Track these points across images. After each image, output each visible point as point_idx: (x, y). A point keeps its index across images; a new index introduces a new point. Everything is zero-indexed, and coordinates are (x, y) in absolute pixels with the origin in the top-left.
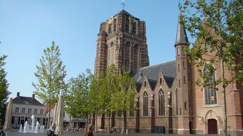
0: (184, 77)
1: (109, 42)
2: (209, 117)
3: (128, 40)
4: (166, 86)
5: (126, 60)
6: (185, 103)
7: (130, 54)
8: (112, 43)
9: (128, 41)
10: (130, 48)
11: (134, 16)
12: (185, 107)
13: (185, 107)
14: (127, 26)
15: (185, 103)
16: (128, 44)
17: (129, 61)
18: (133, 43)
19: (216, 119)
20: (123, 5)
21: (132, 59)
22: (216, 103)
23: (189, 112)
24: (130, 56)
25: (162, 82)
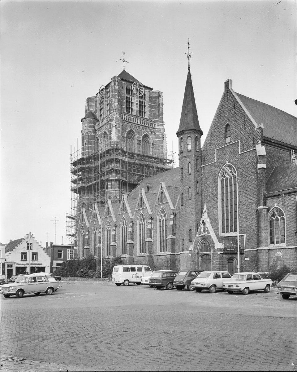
20: (124, 61)
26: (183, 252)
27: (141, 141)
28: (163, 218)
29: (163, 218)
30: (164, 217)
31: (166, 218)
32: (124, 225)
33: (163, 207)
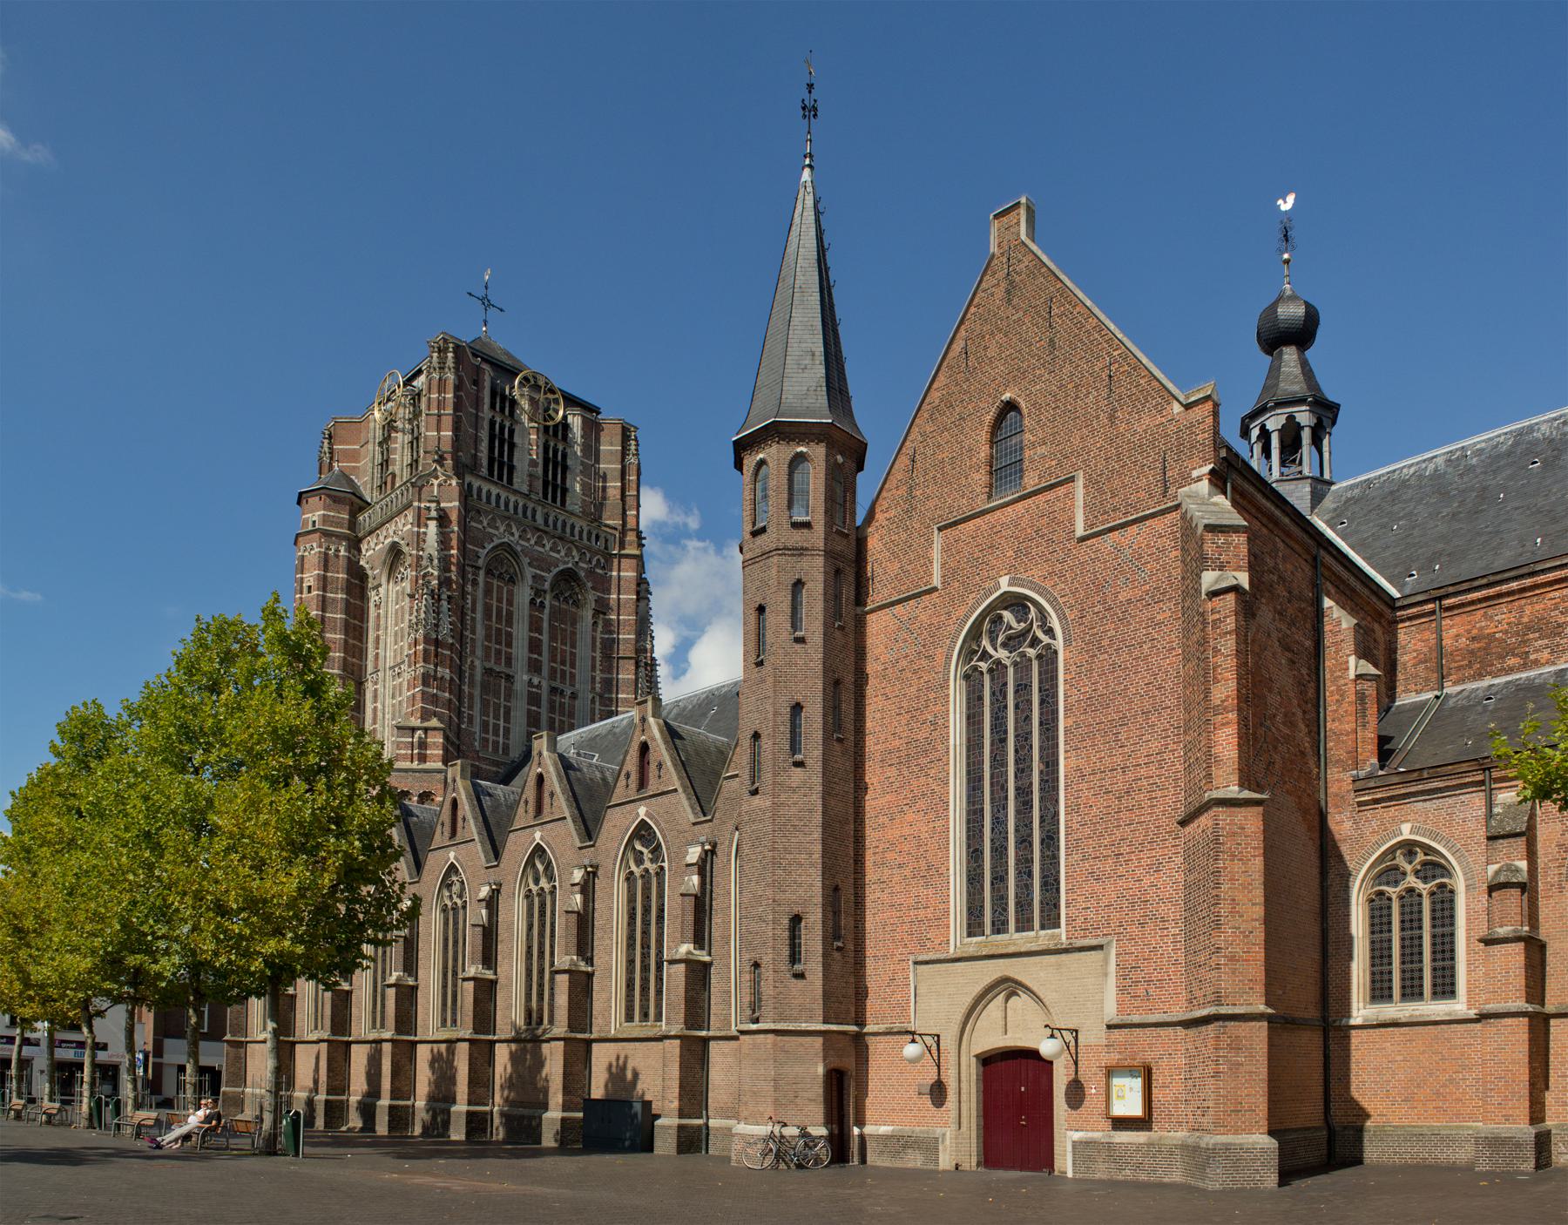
0: (797, 708)
1: (372, 551)
2: (990, 1035)
3: (502, 534)
4: (683, 806)
5: (488, 672)
6: (796, 920)
7: (521, 632)
8: (395, 552)
9: (508, 547)
10: (523, 594)
11: (557, 383)
14: (504, 441)
15: (796, 920)
16: (503, 566)
17: (509, 678)
18: (540, 562)
19: (1047, 1048)
21: (534, 667)
22: (1051, 920)
23: (827, 995)
24: (520, 650)
25: (652, 770)
26: (754, 1027)
27: (545, 592)
28: (647, 864)
29: (647, 864)
30: (652, 861)
31: (662, 868)
32: (451, 897)
33: (647, 814)
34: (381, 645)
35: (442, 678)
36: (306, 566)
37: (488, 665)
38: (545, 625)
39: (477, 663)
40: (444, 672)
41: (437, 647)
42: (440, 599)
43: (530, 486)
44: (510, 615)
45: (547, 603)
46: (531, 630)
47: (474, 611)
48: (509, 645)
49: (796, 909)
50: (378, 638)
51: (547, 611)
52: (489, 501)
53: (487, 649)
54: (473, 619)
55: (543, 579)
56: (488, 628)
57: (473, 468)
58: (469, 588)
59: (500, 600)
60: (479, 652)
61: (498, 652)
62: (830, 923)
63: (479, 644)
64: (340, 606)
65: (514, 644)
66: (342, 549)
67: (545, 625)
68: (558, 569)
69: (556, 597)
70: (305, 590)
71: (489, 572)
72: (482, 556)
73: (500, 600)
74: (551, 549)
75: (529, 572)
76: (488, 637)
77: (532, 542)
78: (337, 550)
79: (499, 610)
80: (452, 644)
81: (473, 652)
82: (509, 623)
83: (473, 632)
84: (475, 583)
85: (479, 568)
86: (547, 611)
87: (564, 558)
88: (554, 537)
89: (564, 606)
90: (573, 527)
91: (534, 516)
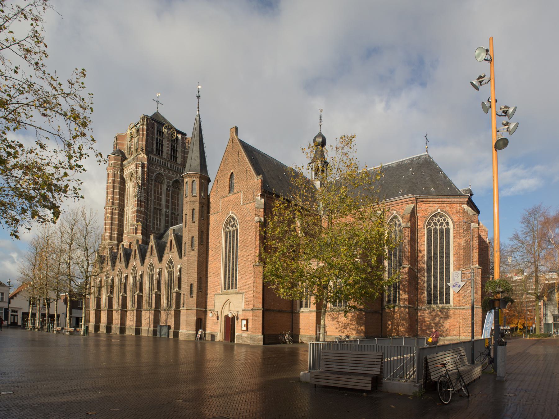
1: (126, 172)
3: (159, 170)
6: (191, 284)
7: (164, 197)
10: (164, 187)
12: (191, 293)
13: (191, 293)
15: (191, 284)
16: (159, 179)
18: (169, 178)
24: (163, 202)
27: (170, 186)
28: (171, 269)
34: (128, 200)
35: (142, 211)
36: (109, 176)
37: (155, 206)
38: (170, 195)
39: (152, 206)
40: (142, 209)
41: (141, 202)
42: (141, 189)
43: (167, 156)
44: (161, 192)
45: (171, 189)
46: (166, 197)
47: (151, 192)
48: (161, 201)
49: (192, 282)
50: (127, 197)
51: (171, 191)
52: (155, 161)
53: (155, 202)
54: (151, 194)
55: (170, 183)
56: (155, 196)
57: (151, 152)
58: (150, 185)
59: (158, 188)
60: (152, 203)
61: (158, 203)
62: (199, 286)
63: (152, 201)
64: (118, 188)
65: (162, 201)
66: (119, 172)
67: (170, 195)
68: (174, 180)
69: (173, 187)
70: (109, 183)
71: (155, 181)
72: (154, 177)
73: (158, 188)
74: (172, 174)
75: (166, 181)
76: (155, 199)
77: (167, 172)
78: (117, 172)
79: (158, 191)
80: (145, 201)
81: (151, 203)
82: (161, 195)
83: (151, 198)
84: (151, 184)
85: (153, 180)
86: (171, 191)
87: (176, 177)
88: (173, 171)
89: (176, 190)
90: (178, 168)
91: (167, 166)
